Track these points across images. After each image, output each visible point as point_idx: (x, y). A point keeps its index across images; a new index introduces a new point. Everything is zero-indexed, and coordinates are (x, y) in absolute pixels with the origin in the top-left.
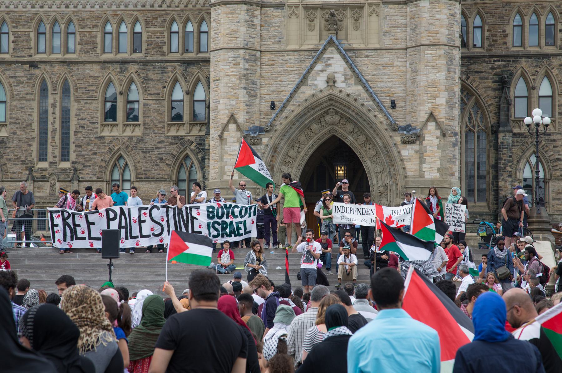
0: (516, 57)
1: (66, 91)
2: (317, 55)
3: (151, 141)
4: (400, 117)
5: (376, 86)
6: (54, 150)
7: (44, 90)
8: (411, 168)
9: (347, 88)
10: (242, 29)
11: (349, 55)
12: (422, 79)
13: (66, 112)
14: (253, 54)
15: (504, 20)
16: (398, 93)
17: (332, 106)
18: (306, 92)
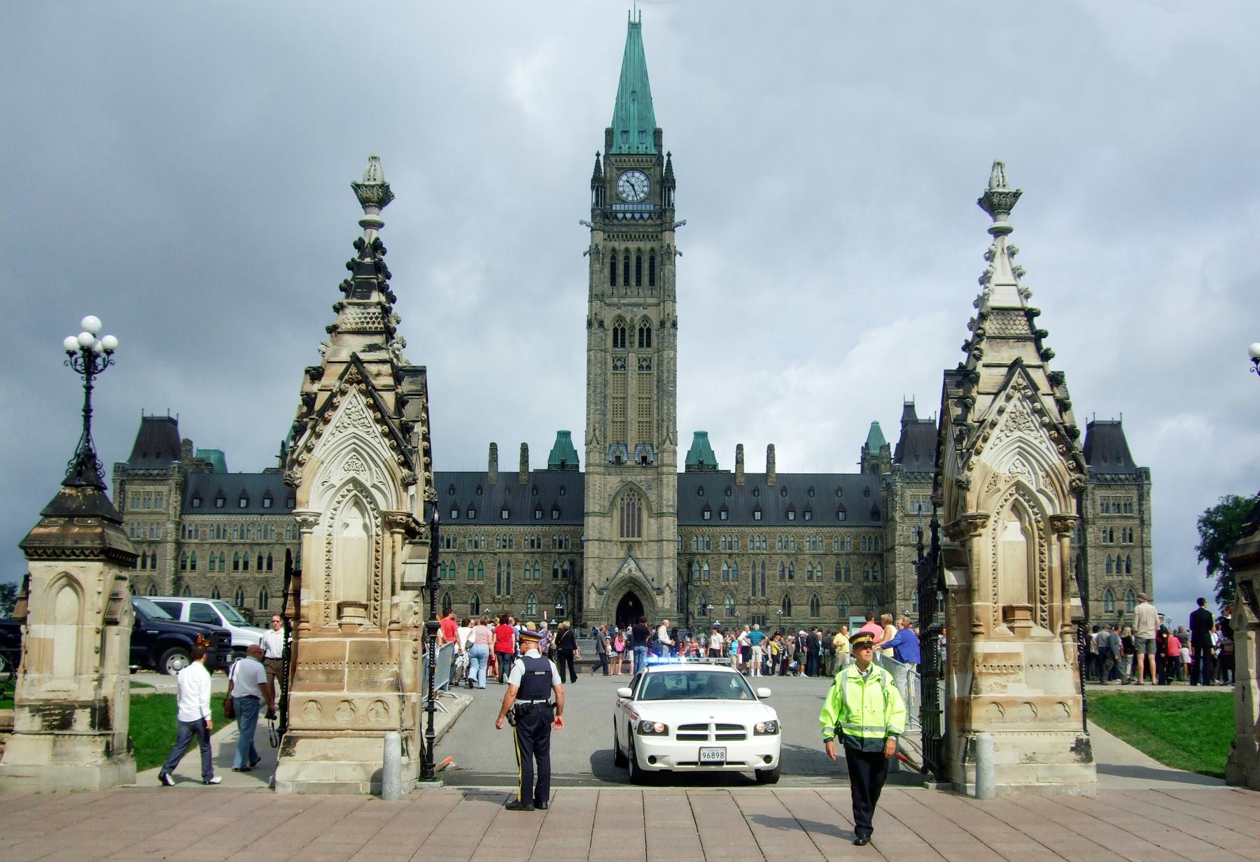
0: (695, 554)
1: (509, 565)
2: (625, 560)
3: (545, 587)
4: (655, 585)
5: (647, 572)
6: (503, 590)
7: (499, 565)
8: (660, 604)
9: (636, 573)
10: (597, 551)
11: (636, 560)
12: (664, 571)
13: (509, 574)
14: (601, 559)
15: (690, 539)
16: (655, 575)
17: (632, 580)
18: (621, 575)
